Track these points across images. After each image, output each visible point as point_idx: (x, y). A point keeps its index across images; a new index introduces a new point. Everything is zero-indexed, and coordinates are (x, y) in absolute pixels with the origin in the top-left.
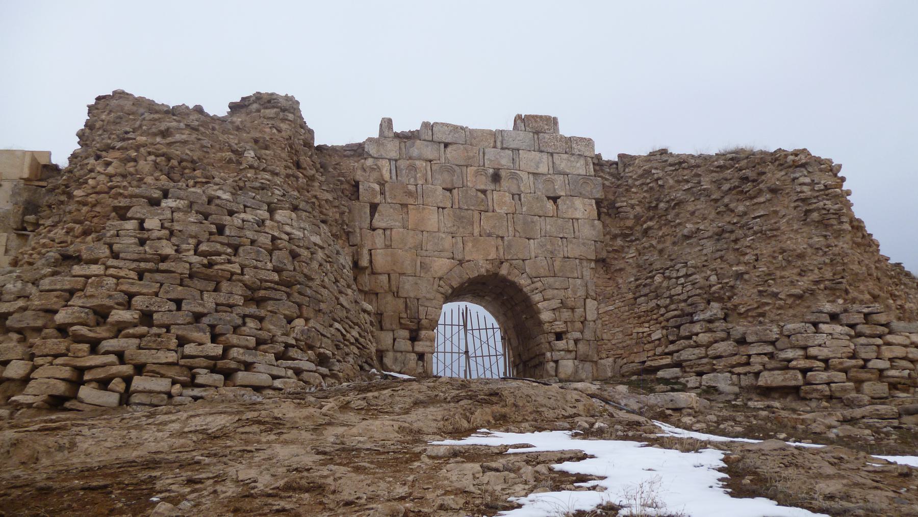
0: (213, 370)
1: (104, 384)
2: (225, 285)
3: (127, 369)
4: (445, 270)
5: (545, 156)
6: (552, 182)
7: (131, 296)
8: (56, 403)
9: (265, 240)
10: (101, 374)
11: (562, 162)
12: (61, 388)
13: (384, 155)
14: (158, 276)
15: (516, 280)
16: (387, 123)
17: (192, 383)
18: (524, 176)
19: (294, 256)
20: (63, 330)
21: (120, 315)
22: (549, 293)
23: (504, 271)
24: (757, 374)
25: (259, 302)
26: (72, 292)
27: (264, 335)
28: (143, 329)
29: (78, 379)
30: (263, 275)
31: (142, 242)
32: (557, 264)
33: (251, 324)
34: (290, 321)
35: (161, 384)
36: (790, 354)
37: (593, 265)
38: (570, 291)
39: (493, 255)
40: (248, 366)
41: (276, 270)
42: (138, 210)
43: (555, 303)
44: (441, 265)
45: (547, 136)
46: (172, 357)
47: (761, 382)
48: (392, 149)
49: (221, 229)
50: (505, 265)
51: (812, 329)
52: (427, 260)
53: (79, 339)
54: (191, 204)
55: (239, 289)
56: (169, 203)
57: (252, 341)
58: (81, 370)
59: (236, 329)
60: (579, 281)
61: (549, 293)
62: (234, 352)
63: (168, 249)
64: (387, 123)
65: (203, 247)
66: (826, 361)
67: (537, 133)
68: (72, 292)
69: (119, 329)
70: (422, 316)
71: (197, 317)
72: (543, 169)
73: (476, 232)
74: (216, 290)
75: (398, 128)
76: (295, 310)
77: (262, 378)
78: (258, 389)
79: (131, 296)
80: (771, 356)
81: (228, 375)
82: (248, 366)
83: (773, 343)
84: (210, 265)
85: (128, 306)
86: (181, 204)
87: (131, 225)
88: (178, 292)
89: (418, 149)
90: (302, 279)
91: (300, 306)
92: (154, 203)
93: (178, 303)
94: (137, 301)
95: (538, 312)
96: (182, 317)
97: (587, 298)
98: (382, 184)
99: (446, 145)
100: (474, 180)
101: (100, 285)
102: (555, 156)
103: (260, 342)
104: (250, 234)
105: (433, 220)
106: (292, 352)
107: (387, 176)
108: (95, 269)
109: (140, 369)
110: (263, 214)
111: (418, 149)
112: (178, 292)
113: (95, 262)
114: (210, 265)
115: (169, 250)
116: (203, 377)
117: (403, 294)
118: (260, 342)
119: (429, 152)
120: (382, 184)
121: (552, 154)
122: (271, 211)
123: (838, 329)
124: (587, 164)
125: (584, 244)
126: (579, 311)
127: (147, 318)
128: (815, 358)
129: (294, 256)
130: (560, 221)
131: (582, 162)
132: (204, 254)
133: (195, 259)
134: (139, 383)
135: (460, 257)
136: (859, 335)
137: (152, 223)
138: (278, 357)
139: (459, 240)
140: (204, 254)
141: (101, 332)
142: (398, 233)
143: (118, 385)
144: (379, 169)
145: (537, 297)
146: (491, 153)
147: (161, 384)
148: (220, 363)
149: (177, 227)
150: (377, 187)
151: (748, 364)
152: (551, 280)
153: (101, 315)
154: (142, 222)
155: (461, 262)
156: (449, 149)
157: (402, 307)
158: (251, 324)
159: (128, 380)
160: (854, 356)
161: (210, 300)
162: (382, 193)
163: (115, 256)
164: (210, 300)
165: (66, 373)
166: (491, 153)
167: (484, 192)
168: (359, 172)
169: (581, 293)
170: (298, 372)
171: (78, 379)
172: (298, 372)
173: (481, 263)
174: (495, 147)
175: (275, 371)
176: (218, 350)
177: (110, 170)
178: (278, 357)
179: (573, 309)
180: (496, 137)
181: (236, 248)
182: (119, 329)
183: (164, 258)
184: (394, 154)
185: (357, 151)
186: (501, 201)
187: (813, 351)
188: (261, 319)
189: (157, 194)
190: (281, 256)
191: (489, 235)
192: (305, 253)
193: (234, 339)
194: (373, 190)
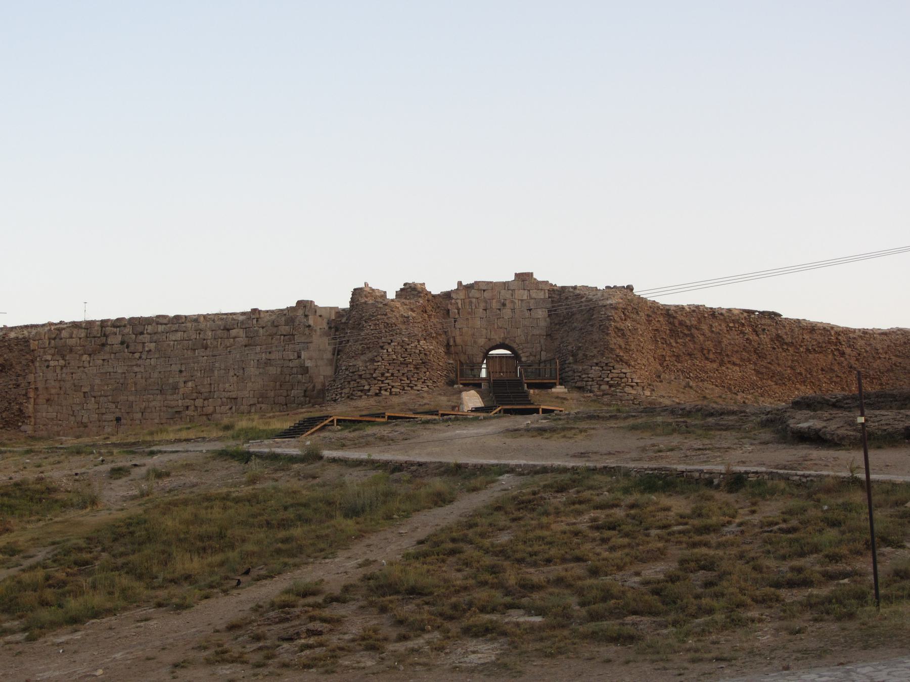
0: (408, 386)
1: (386, 390)
2: (409, 365)
3: (390, 387)
4: (483, 343)
5: (526, 292)
6: (529, 302)
7: (388, 370)
8: (377, 395)
9: (417, 351)
10: (385, 388)
11: (534, 294)
12: (378, 391)
13: (459, 297)
14: (394, 364)
15: (512, 345)
16: (460, 283)
17: (404, 390)
18: (516, 301)
19: (425, 354)
20: (375, 378)
21: (387, 375)
22: (525, 350)
23: (507, 342)
24: (576, 382)
25: (417, 369)
26: (375, 370)
27: (419, 377)
28: (392, 378)
29: (380, 389)
30: (418, 361)
31: (388, 355)
32: (529, 338)
33: (416, 375)
34: (425, 373)
35: (398, 390)
36: (584, 376)
37: (545, 337)
38: (534, 350)
39: (502, 336)
40: (416, 385)
41: (421, 360)
42: (386, 346)
43: (528, 354)
44: (482, 341)
45: (527, 282)
46: (399, 384)
47: (577, 385)
48: (462, 295)
49: (406, 349)
50: (508, 340)
51: (590, 368)
52: (476, 340)
53: (379, 380)
54: (398, 343)
55: (412, 366)
56: (393, 344)
57: (416, 379)
58: (381, 387)
59: (412, 376)
60: (538, 345)
61: (525, 350)
62: (413, 382)
63: (395, 357)
64: (460, 283)
65: (403, 356)
66: (592, 378)
67: (523, 281)
68: (375, 370)
69: (387, 378)
70: (475, 361)
71: (403, 374)
72: (525, 297)
73: (496, 327)
74: (407, 367)
75: (464, 283)
76: (426, 370)
77: (419, 388)
78: (418, 391)
79: (388, 370)
80: (580, 376)
81: (412, 387)
82: (416, 385)
83: (580, 372)
84: (405, 360)
85: (388, 372)
86: (396, 344)
87: (385, 351)
88: (399, 368)
89: (474, 293)
90: (427, 361)
91: (427, 369)
92: (389, 344)
93: (399, 371)
94: (390, 371)
95: (521, 358)
96: (400, 374)
97: (542, 350)
98: (458, 309)
99: (484, 291)
100: (495, 305)
101: (381, 368)
102: (531, 291)
103: (418, 379)
104: (413, 350)
105: (478, 323)
106: (426, 381)
107: (460, 306)
108: (379, 363)
109: (393, 387)
110: (416, 343)
111: (474, 293)
112: (399, 368)
113: (378, 362)
114: (405, 360)
115: (395, 357)
116: (406, 388)
117: (467, 353)
118: (418, 379)
119: (477, 295)
120: (458, 309)
121: (529, 290)
122: (419, 341)
123: (597, 368)
124: (545, 293)
125: (541, 329)
126: (538, 357)
127: (392, 375)
128: (589, 377)
129: (425, 354)
130: (531, 320)
131: (543, 292)
132: (404, 358)
133: (402, 359)
134: (393, 390)
135: (489, 337)
136: (603, 370)
137: (390, 350)
138: (423, 383)
139: (489, 331)
140: (404, 358)
141: (383, 379)
142: (465, 330)
143: (389, 390)
144: (457, 303)
145: (520, 352)
146: (503, 292)
147: (398, 390)
148: (410, 385)
149: (396, 351)
150: (456, 311)
151: (574, 379)
152: (526, 345)
153: (383, 374)
154: (387, 350)
155: (489, 340)
156: (485, 293)
157: (467, 358)
158: (416, 375)
159: (390, 389)
160: (600, 377)
161: (406, 370)
162: (458, 313)
163: (383, 360)
164: (406, 370)
165: (379, 388)
166: (503, 292)
167: (499, 309)
168: (449, 305)
169: (539, 349)
170: (428, 386)
171: (380, 389)
172: (428, 386)
173: (498, 339)
174: (505, 289)
175: (422, 386)
176: (409, 382)
177: (372, 328)
178: (423, 383)
179: (535, 356)
180: (505, 285)
181: (410, 355)
182: (387, 378)
183: (394, 359)
184: (463, 297)
185: (447, 295)
186: (507, 313)
187: (589, 375)
188: (418, 373)
189: (390, 341)
190: (422, 355)
191: (501, 328)
192: (428, 353)
193: (412, 379)
194: (455, 312)
